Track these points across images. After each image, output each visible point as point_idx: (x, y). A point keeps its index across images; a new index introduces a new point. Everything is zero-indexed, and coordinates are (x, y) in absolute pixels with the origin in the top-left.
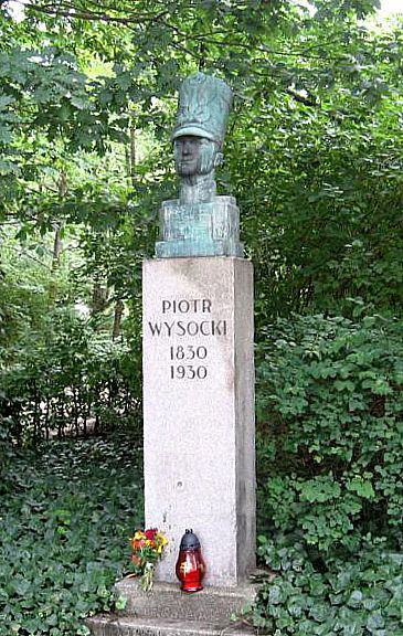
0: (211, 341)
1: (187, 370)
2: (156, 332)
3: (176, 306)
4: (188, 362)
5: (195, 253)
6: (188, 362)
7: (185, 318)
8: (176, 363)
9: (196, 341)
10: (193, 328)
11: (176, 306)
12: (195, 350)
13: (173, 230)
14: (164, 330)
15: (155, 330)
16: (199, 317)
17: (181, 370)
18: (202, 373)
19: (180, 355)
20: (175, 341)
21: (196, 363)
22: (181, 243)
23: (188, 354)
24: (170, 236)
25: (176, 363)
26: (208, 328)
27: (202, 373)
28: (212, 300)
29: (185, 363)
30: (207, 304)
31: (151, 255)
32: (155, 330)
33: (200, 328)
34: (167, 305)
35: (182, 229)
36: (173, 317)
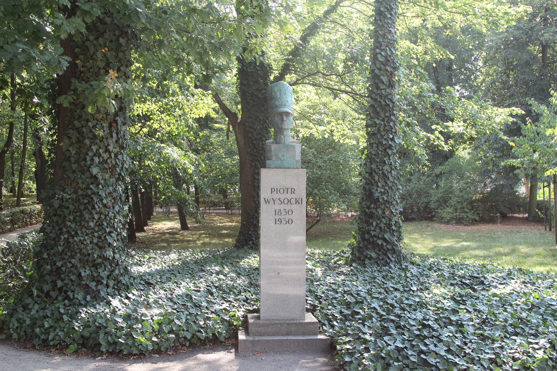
0: (295, 207)
1: (283, 220)
3: (278, 191)
4: (284, 217)
5: (286, 166)
6: (284, 217)
7: (282, 197)
8: (278, 217)
9: (288, 207)
10: (286, 201)
11: (278, 191)
13: (276, 155)
14: (272, 202)
15: (267, 201)
16: (289, 196)
18: (290, 222)
20: (277, 207)
21: (287, 217)
22: (279, 162)
24: (274, 158)
25: (278, 217)
26: (293, 201)
27: (290, 222)
28: (295, 188)
30: (293, 190)
31: (264, 166)
32: (267, 201)
33: (289, 201)
35: (280, 155)
36: (276, 196)
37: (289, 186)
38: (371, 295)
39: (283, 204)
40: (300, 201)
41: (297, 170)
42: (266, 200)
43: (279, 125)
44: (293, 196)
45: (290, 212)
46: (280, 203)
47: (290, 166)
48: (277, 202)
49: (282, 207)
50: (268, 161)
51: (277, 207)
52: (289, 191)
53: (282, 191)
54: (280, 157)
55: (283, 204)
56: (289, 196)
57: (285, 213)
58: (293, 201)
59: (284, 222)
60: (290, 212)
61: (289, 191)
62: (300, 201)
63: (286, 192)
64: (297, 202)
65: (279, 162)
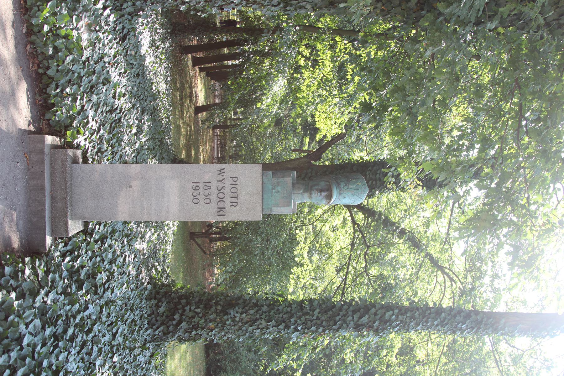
0: (214, 206)
1: (197, 192)
2: (219, 172)
4: (202, 193)
5: (265, 196)
6: (202, 193)
7: (227, 191)
9: (214, 198)
10: (221, 195)
12: (209, 197)
13: (278, 183)
14: (220, 178)
15: (221, 172)
16: (228, 200)
17: (197, 188)
18: (195, 201)
19: (206, 188)
20: (214, 185)
21: (201, 197)
22: (270, 187)
23: (207, 193)
24: (275, 181)
25: (201, 185)
26: (221, 205)
27: (195, 201)
28: (238, 207)
29: (201, 190)
30: (235, 204)
32: (221, 172)
33: (221, 200)
34: (235, 179)
35: (279, 188)
36: (228, 183)
37: (242, 199)
38: (107, 304)
39: (218, 192)
40: (222, 213)
41: (260, 209)
42: (223, 171)
43: (316, 187)
44: (228, 204)
45: (207, 201)
46: (219, 188)
47: (265, 200)
48: (221, 185)
49: (214, 191)
50: (271, 173)
51: (214, 185)
52: (234, 200)
53: (234, 190)
54: (277, 188)
55: (218, 192)
56: (228, 200)
57: (206, 194)
58: (221, 205)
59: (195, 193)
60: (207, 201)
61: (234, 200)
62: (222, 213)
63: (233, 195)
64: (221, 209)
65: (270, 187)
